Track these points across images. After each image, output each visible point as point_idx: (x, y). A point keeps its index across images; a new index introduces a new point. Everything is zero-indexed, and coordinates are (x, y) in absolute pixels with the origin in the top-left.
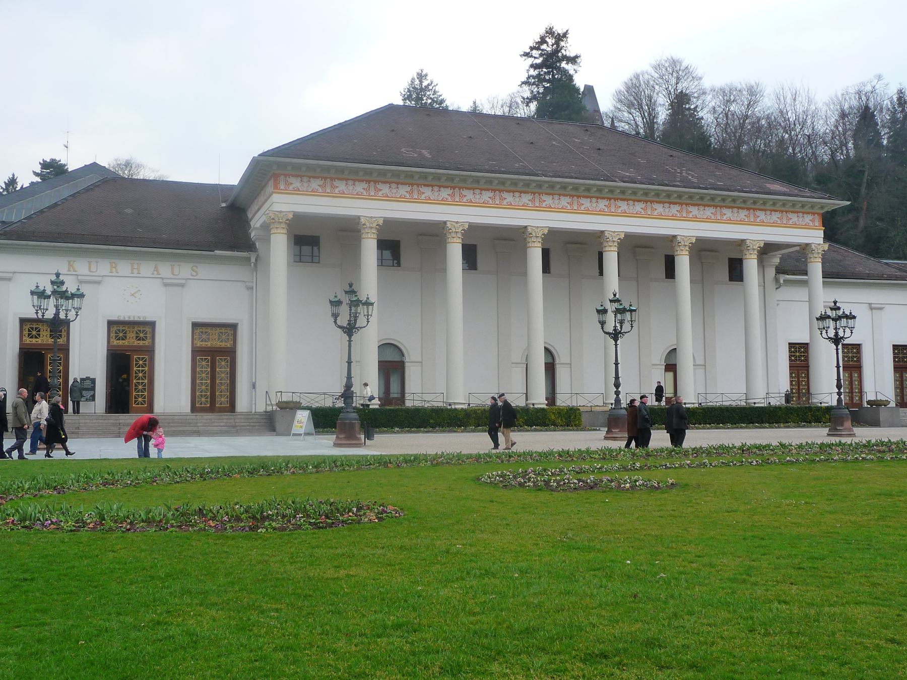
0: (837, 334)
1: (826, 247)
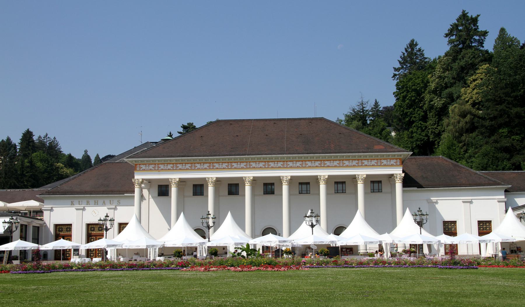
0: (312, 223)
1: (403, 175)
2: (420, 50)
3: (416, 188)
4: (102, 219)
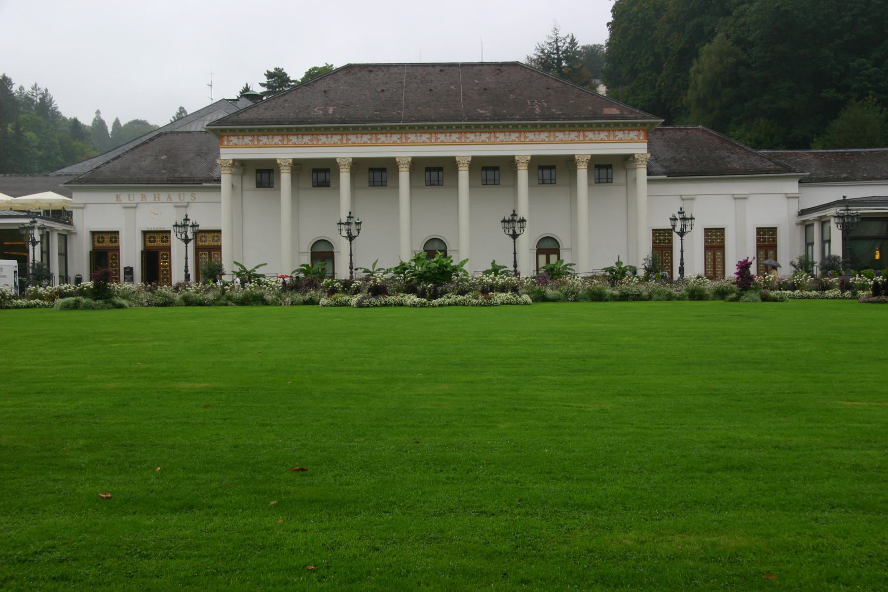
0: (514, 231)
3: (665, 177)
4: (179, 224)
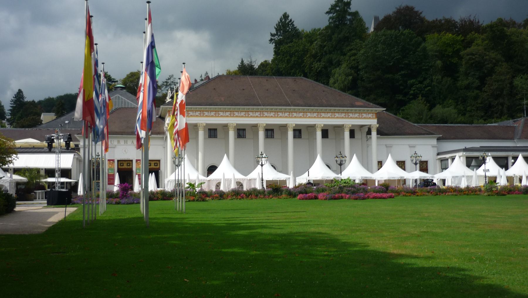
1: (378, 126)
2: (291, 20)
